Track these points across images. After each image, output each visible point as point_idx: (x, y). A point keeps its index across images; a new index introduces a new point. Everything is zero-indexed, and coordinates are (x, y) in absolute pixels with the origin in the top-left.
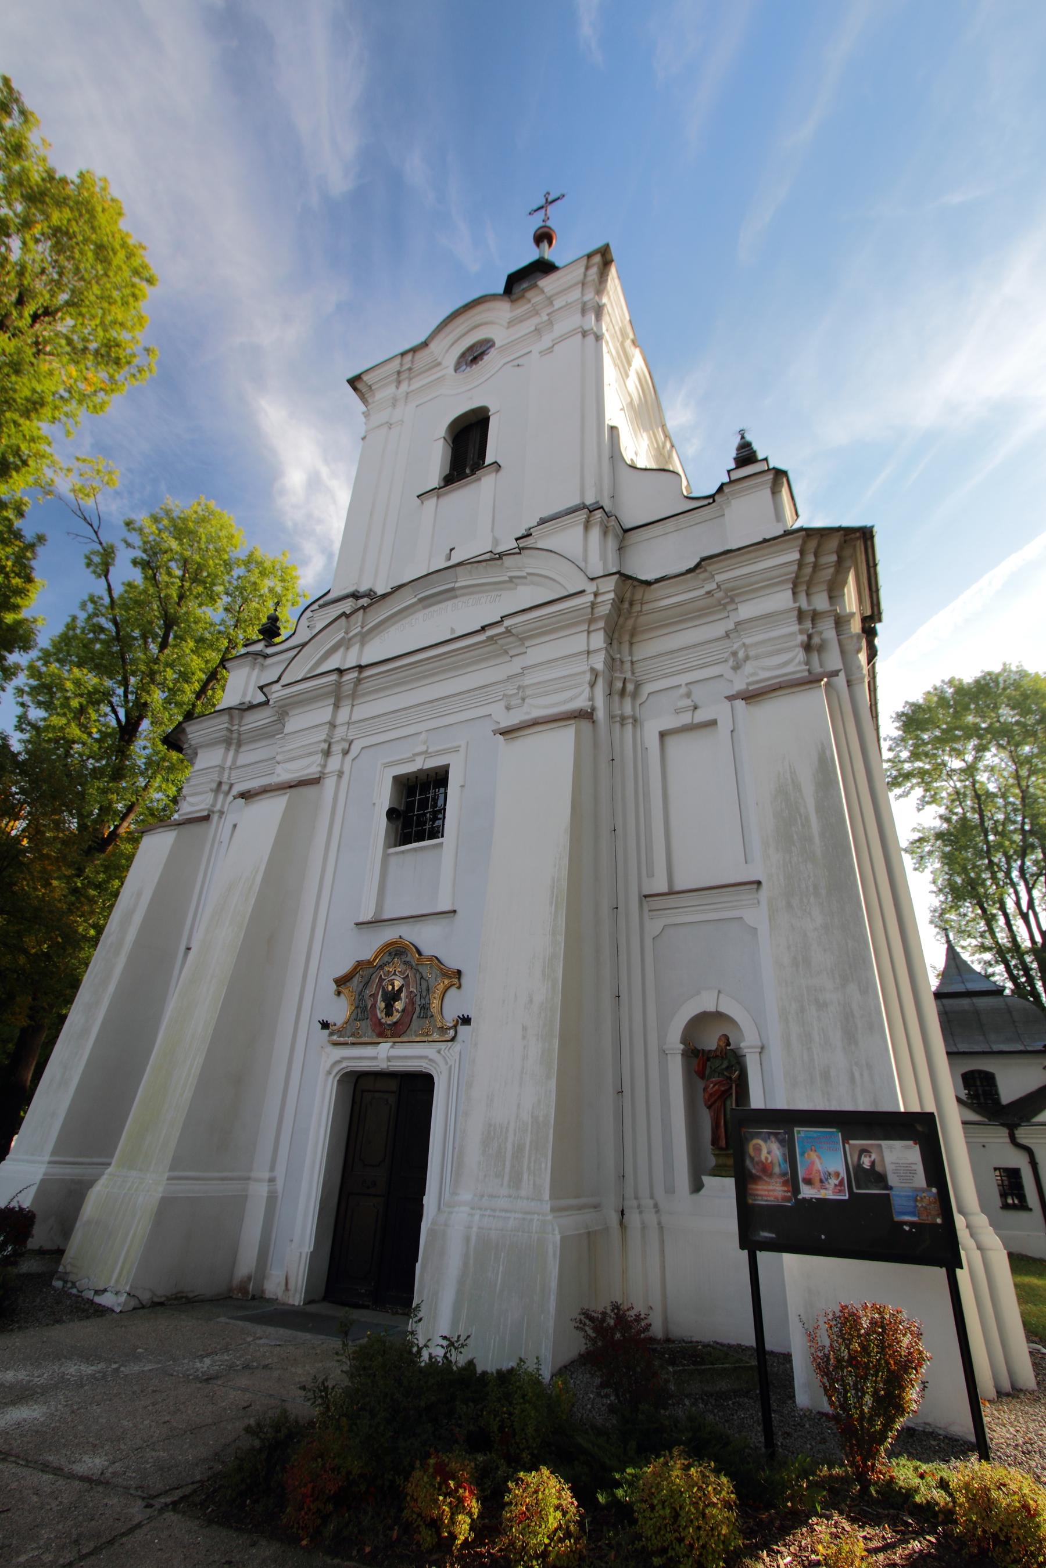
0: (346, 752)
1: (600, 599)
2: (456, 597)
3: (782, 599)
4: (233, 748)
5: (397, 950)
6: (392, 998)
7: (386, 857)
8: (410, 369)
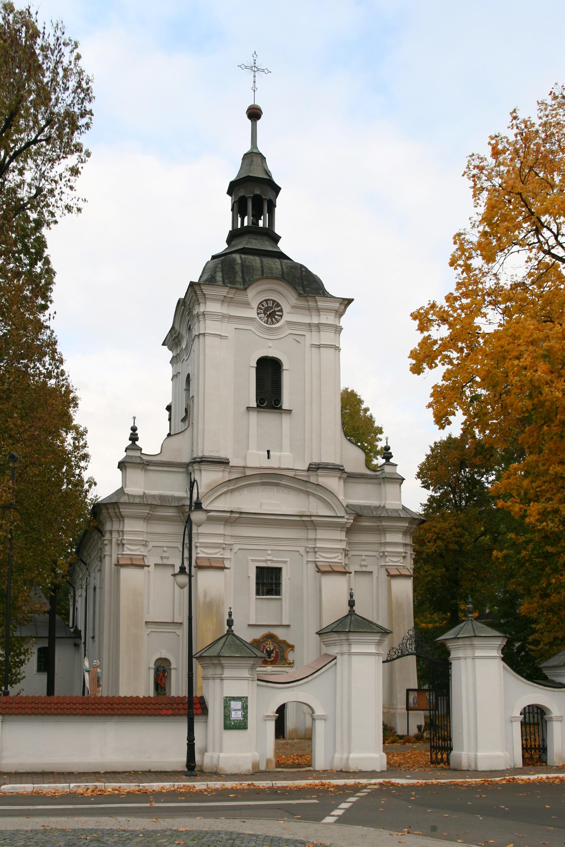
0: (231, 550)
5: (271, 637)
8: (232, 298)
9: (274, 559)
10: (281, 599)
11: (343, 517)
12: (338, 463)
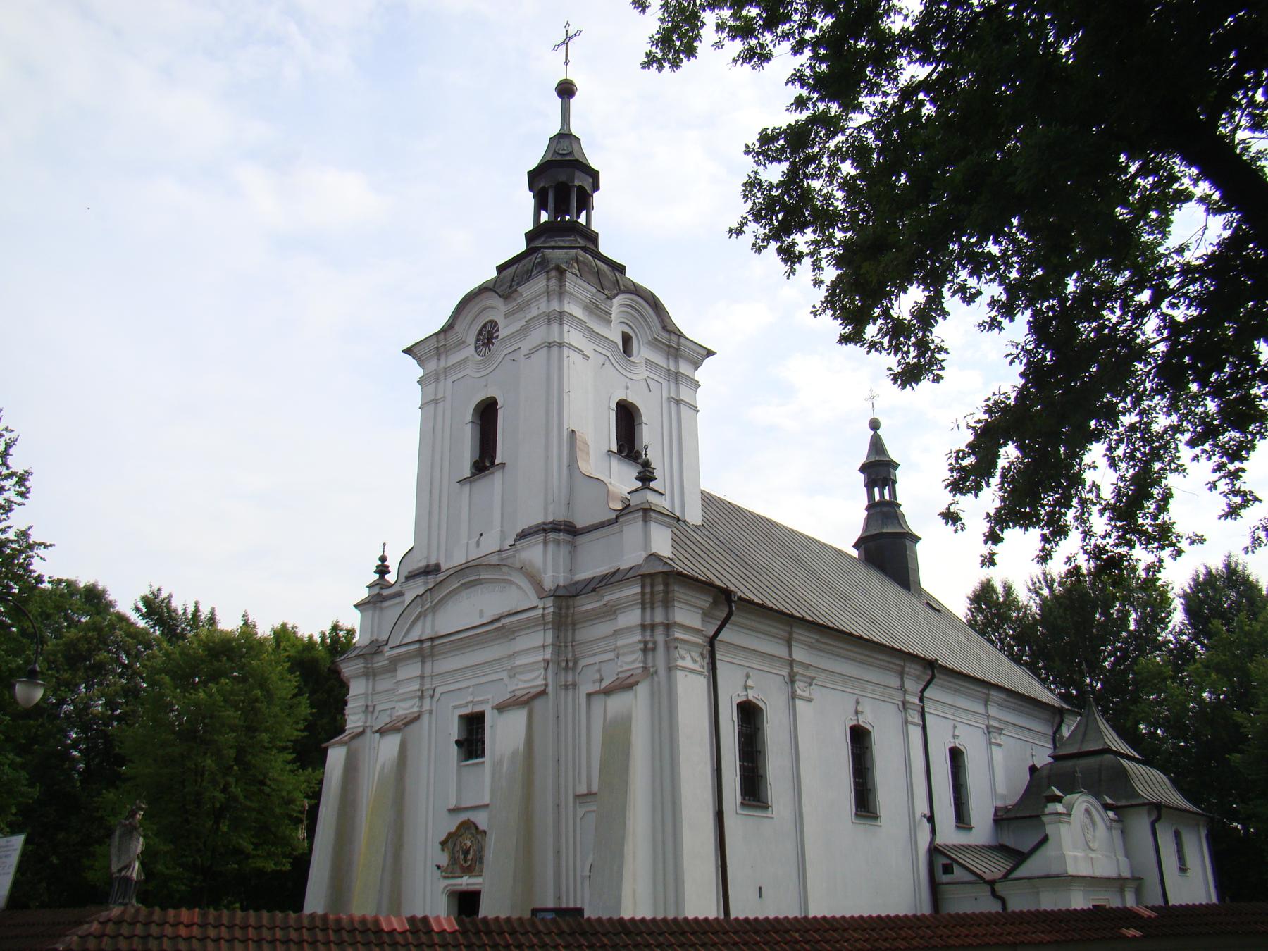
0: (432, 696)
1: (546, 611)
2: (482, 584)
3: (632, 617)
4: (371, 678)
6: (466, 852)
7: (459, 767)
8: (445, 345)
9: (475, 700)
10: (483, 762)
11: (535, 608)
12: (550, 519)
